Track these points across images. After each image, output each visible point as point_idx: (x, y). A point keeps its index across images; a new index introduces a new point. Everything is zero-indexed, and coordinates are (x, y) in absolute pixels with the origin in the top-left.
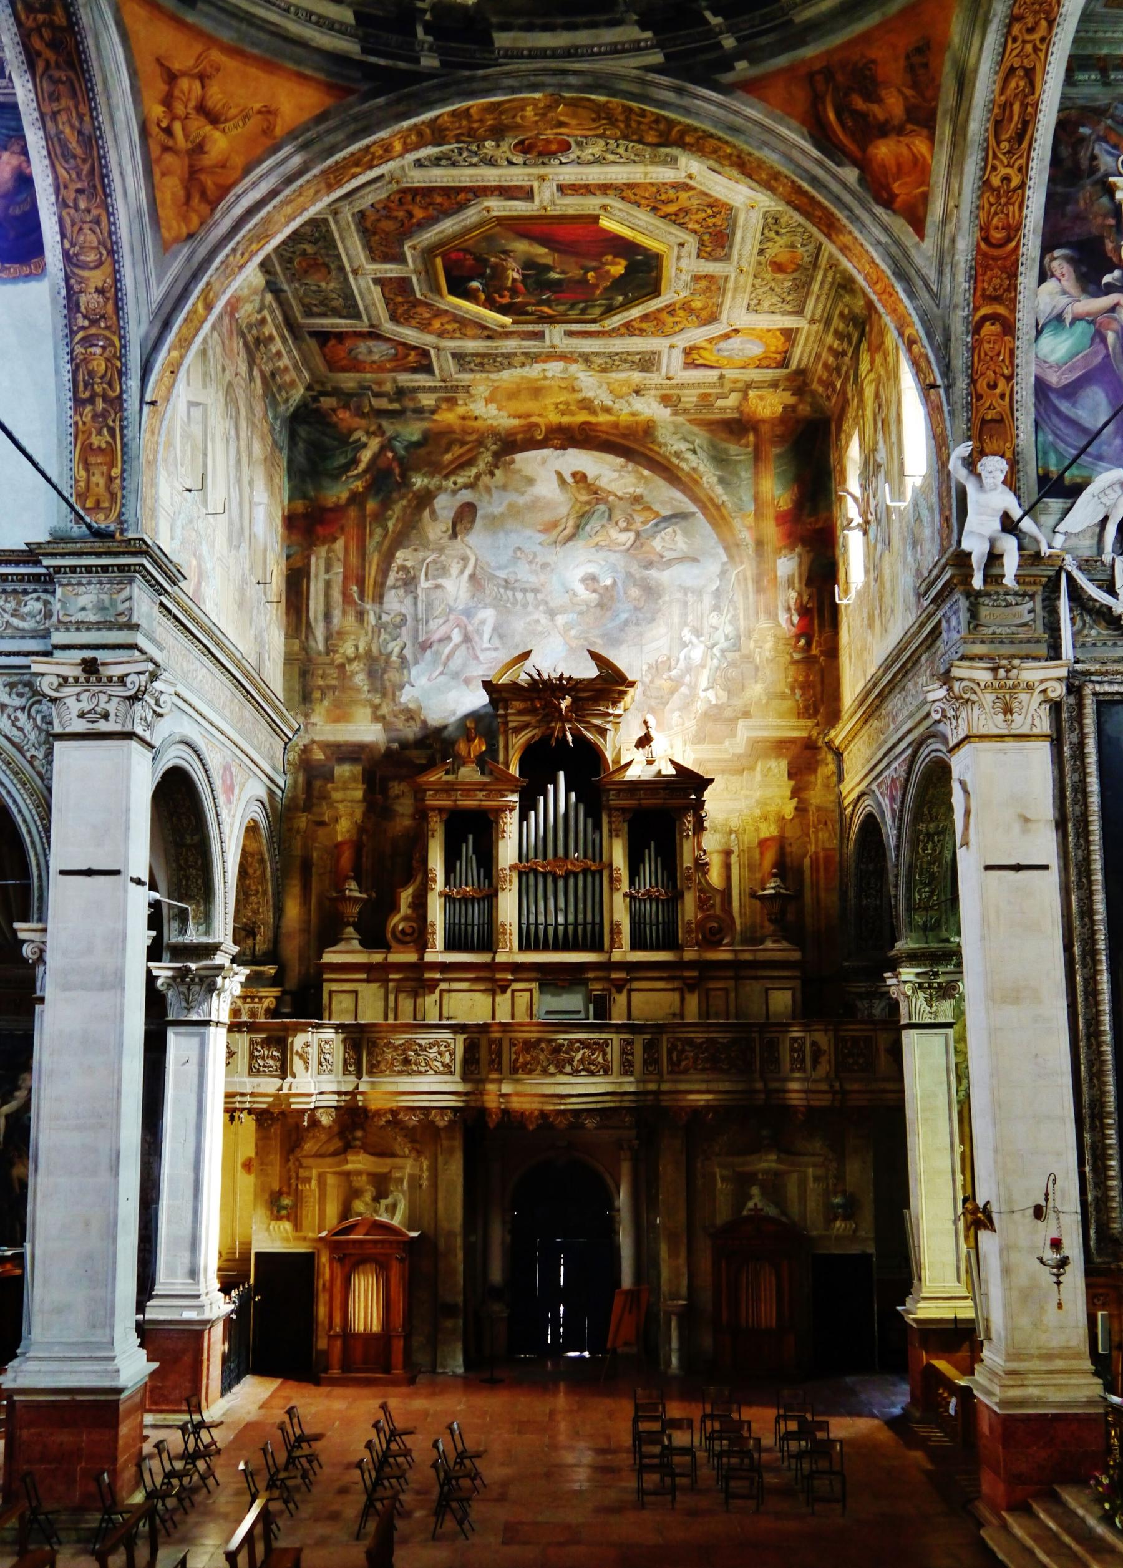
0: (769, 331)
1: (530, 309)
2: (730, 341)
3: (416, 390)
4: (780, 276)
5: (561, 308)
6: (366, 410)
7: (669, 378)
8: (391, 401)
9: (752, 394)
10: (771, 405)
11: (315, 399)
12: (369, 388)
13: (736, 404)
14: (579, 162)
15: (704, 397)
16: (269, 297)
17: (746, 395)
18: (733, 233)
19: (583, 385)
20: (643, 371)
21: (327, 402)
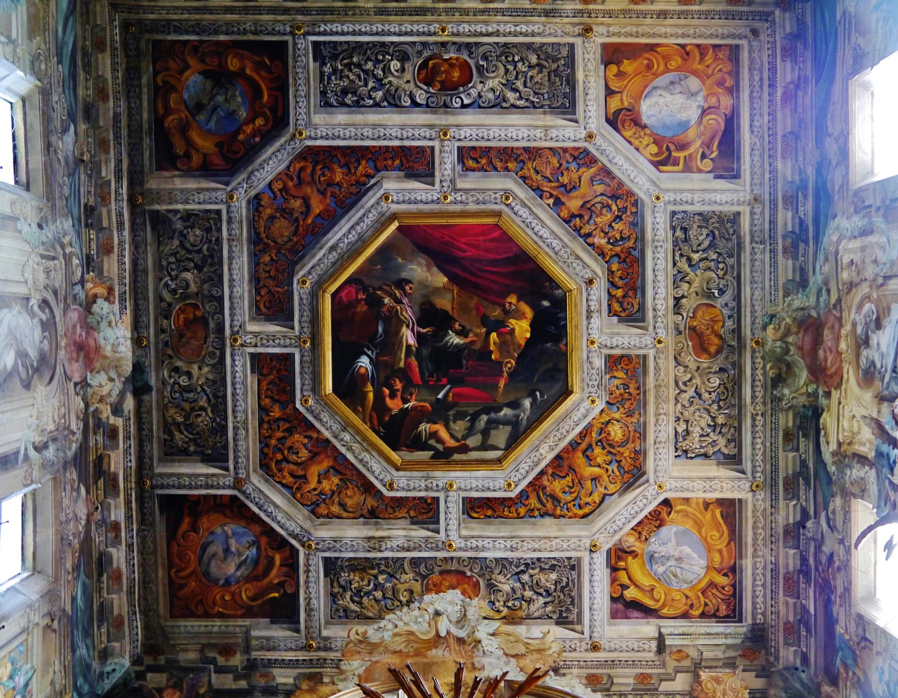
0: (707, 505)
1: (424, 427)
2: (664, 530)
3: (271, 663)
4: (705, 362)
5: (459, 427)
6: (202, 691)
7: (595, 648)
8: (237, 678)
9: (704, 675)
10: (732, 689)
11: (141, 676)
12: (213, 661)
13: (687, 688)
14: (477, 105)
15: (643, 678)
16: (129, 403)
17: (697, 676)
18: (643, 252)
19: (486, 661)
20: (562, 622)
21: (155, 679)
